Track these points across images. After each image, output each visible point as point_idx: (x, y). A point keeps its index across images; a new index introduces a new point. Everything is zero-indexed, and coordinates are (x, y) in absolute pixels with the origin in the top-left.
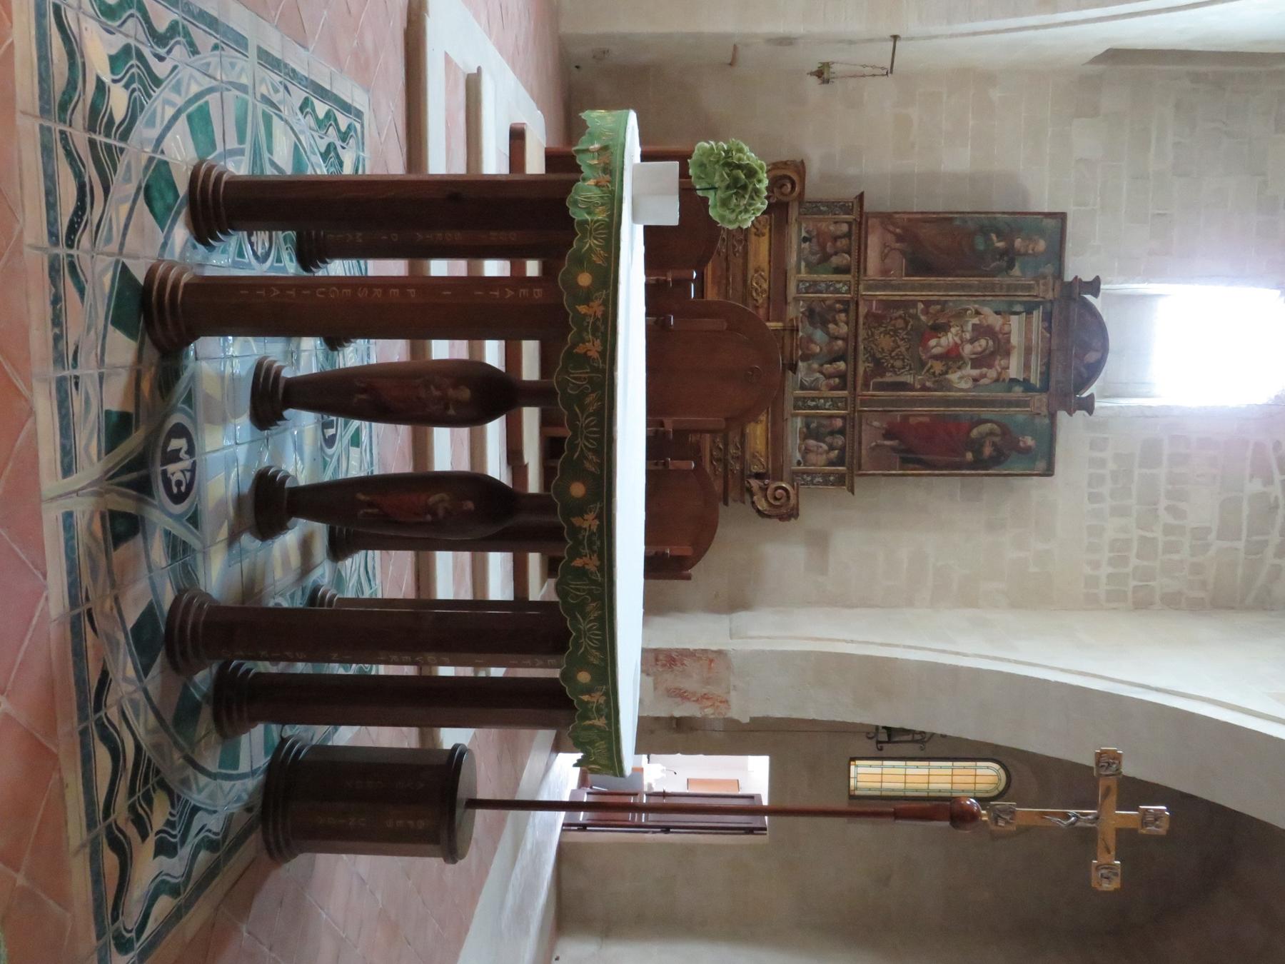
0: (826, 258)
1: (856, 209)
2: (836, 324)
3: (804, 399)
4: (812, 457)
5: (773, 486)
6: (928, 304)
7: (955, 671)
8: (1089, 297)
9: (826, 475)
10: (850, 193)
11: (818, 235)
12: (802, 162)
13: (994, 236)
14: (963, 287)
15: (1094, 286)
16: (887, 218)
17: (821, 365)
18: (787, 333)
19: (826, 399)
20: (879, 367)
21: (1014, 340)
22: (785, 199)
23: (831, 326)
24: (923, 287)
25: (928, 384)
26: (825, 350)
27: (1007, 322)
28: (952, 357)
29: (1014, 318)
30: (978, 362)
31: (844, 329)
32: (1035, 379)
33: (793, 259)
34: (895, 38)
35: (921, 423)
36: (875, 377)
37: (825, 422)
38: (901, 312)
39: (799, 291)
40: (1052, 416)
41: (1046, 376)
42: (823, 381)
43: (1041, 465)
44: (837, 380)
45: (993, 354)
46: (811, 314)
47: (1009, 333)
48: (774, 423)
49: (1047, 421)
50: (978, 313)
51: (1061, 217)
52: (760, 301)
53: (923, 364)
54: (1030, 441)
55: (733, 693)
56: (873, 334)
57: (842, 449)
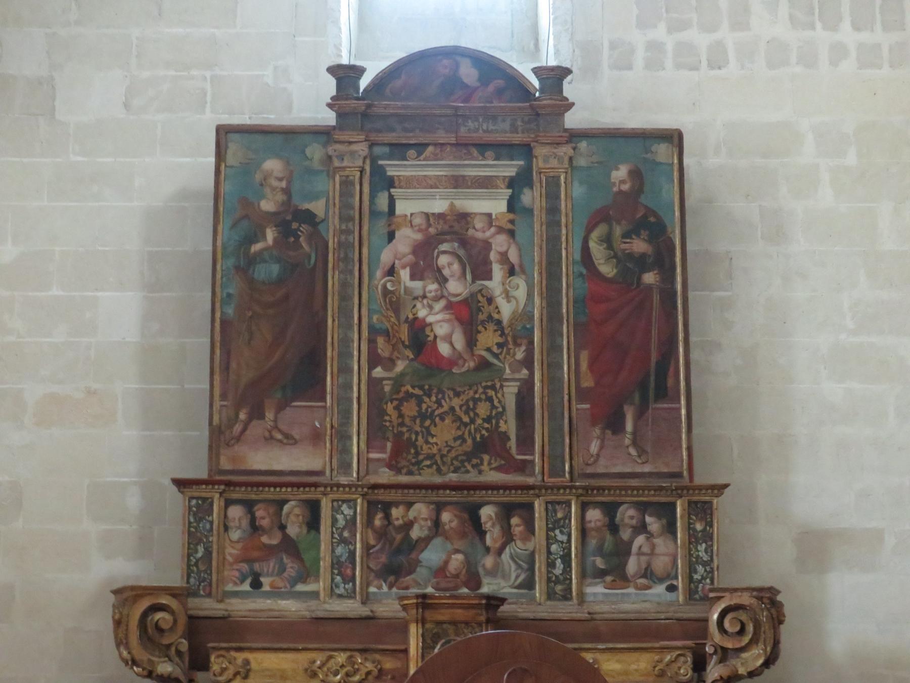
0: (289, 546)
1: (203, 492)
2: (409, 525)
3: (550, 580)
4: (660, 564)
6: (374, 360)
8: (364, 82)
9: (693, 538)
10: (175, 503)
11: (249, 561)
12: (116, 592)
13: (256, 247)
14: (345, 298)
15: (346, 75)
16: (220, 437)
17: (488, 550)
18: (428, 614)
20: (489, 445)
21: (439, 206)
22: (182, 621)
23: (415, 533)
24: (344, 370)
25: (520, 355)
26: (459, 544)
27: (408, 221)
29: (402, 208)
31: (421, 510)
32: (509, 168)
33: (290, 607)
35: (591, 366)
36: (508, 451)
37: (593, 543)
38: (390, 408)
39: (351, 595)
40: (575, 136)
41: (503, 150)
42: (518, 547)
43: (662, 151)
44: (515, 521)
46: (394, 571)
47: (427, 215)
48: (596, 637)
49: (583, 145)
50: (391, 271)
51: (224, 133)
52: (370, 666)
53: (484, 365)
54: (621, 173)
56: (430, 457)
57: (643, 507)
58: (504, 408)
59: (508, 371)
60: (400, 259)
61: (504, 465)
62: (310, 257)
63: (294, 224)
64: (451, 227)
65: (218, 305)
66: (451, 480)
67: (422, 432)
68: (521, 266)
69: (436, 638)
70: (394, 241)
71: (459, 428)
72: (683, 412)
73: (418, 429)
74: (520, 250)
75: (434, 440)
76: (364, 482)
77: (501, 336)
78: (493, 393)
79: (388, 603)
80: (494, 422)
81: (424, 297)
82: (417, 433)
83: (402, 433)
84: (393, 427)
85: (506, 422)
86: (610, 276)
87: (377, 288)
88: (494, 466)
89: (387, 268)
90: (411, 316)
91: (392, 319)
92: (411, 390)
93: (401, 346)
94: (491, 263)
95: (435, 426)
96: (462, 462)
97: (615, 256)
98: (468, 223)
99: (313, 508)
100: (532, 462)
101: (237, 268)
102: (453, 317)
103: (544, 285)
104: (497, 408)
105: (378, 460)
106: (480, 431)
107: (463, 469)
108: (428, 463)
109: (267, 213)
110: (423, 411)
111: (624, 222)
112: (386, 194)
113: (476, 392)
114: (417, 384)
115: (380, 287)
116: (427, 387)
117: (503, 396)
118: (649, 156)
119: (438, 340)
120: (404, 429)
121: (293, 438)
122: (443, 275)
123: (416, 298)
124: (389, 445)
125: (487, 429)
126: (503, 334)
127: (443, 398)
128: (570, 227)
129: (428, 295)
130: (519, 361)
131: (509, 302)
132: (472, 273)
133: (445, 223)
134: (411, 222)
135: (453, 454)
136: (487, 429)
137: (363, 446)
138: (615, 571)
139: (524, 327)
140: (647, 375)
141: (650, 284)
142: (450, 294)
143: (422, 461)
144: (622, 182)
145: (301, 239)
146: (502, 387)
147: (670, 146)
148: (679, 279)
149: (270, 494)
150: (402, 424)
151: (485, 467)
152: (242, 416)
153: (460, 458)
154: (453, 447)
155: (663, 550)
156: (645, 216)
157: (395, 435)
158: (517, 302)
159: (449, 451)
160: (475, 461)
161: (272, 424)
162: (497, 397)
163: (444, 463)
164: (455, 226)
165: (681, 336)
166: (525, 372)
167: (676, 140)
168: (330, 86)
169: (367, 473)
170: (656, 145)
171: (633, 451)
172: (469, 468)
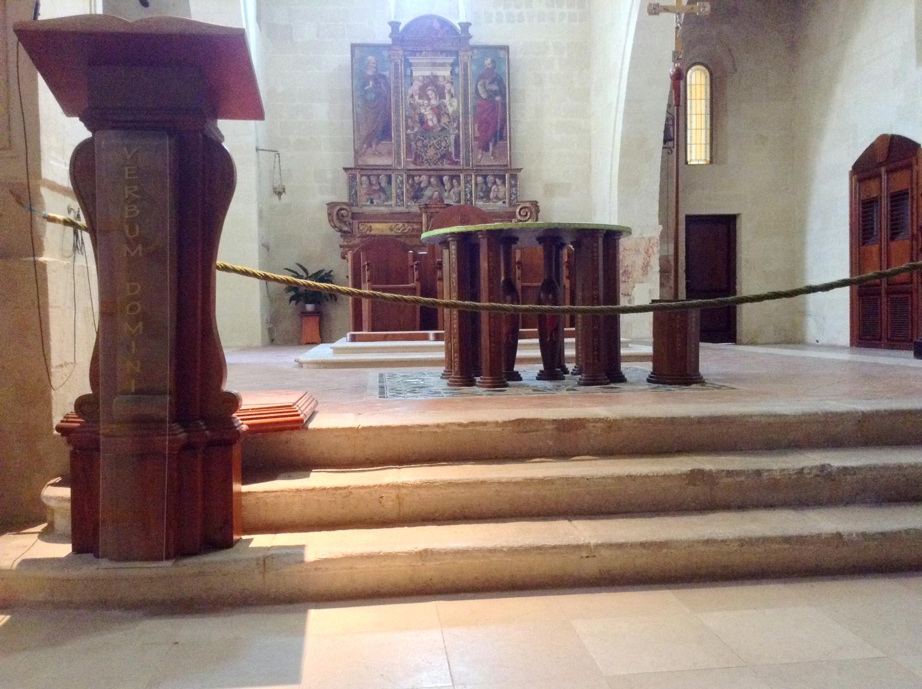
0: (382, 190)
1: (353, 172)
2: (421, 182)
4: (501, 195)
5: (519, 217)
6: (407, 127)
7: (628, 101)
8: (401, 28)
9: (511, 186)
10: (344, 176)
11: (370, 195)
12: (328, 204)
13: (366, 88)
15: (394, 25)
16: (357, 153)
19: (466, 187)
21: (428, 73)
22: (350, 215)
23: (422, 185)
24: (398, 131)
25: (455, 125)
28: (439, 111)
29: (415, 74)
30: (441, 96)
31: (424, 178)
32: (451, 60)
33: (383, 209)
34: (257, 150)
35: (478, 130)
37: (479, 188)
38: (413, 143)
39: (403, 205)
41: (448, 53)
42: (456, 190)
43: (502, 54)
45: (436, 86)
46: (416, 198)
50: (412, 96)
51: (353, 46)
53: (443, 129)
54: (488, 62)
55: (644, 235)
57: (495, 176)
69: (431, 217)
79: (415, 208)
99: (389, 177)
138: (486, 196)
149: (375, 172)
155: (500, 190)
164: (433, 81)
168: (389, 30)
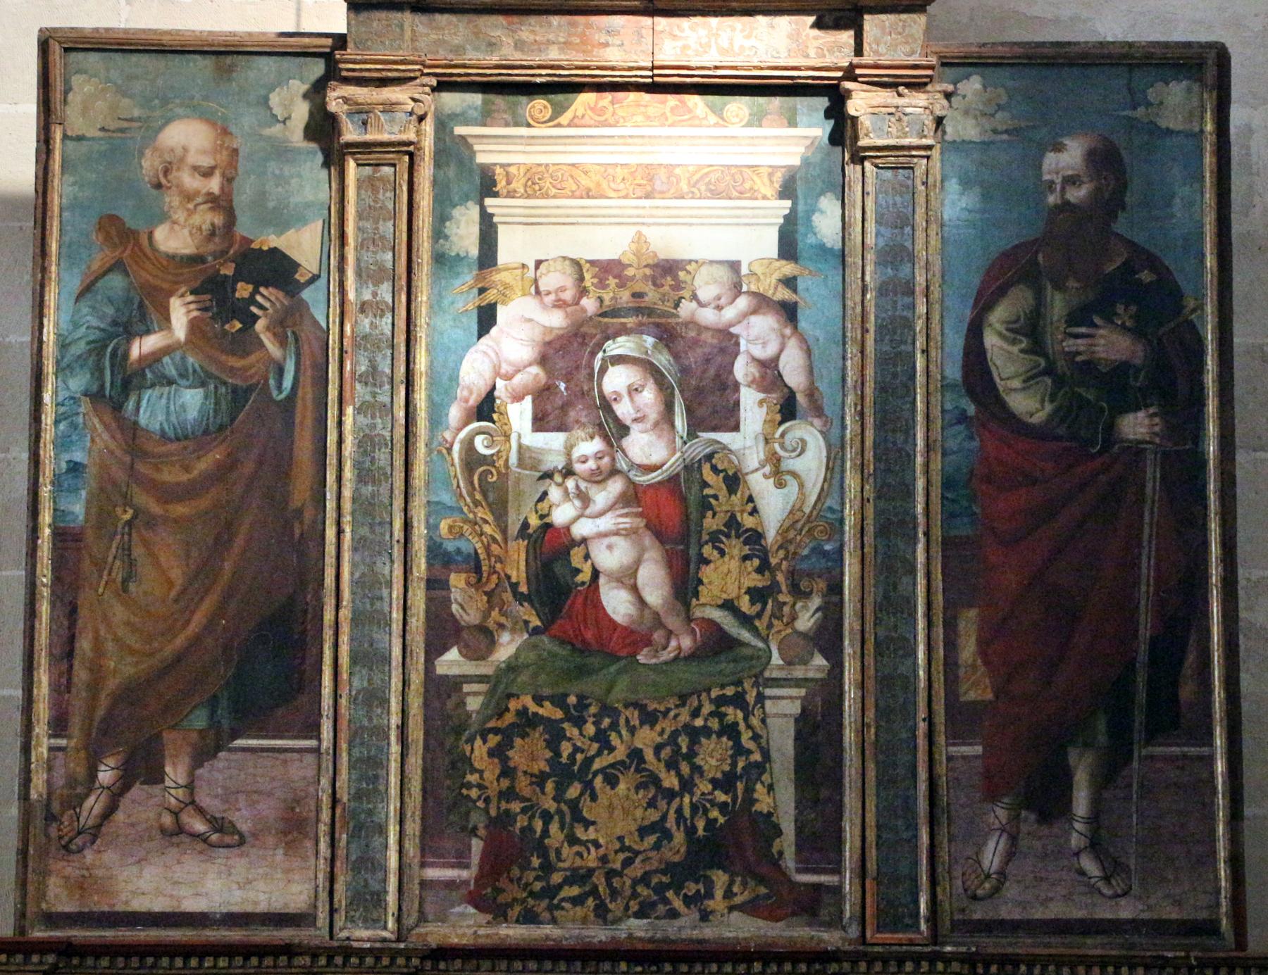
6: (443, 630)
13: (143, 346)
16: (51, 828)
20: (731, 844)
25: (806, 620)
29: (513, 247)
36: (775, 862)
38: (479, 751)
43: (1175, 101)
50: (486, 408)
51: (59, 52)
53: (717, 644)
54: (1070, 156)
56: (579, 876)
58: (766, 755)
59: (776, 659)
60: (508, 377)
61: (768, 897)
62: (280, 371)
63: (240, 285)
64: (637, 295)
65: (46, 491)
66: (630, 936)
67: (559, 811)
68: (812, 393)
70: (494, 331)
71: (652, 804)
72: (1220, 766)
73: (551, 805)
74: (809, 353)
75: (591, 834)
76: (413, 941)
77: (759, 570)
78: (740, 715)
80: (740, 786)
81: (568, 472)
82: (547, 817)
83: (508, 817)
84: (487, 801)
85: (771, 788)
86: (1036, 420)
87: (449, 450)
88: (738, 900)
89: (474, 401)
90: (534, 521)
91: (488, 529)
92: (533, 708)
93: (508, 596)
94: (737, 386)
95: (594, 798)
96: (660, 889)
97: (1049, 371)
98: (678, 286)
100: (837, 890)
101: (96, 396)
102: (641, 523)
103: (869, 442)
104: (749, 752)
105: (450, 885)
106: (706, 811)
107: (661, 909)
108: (575, 891)
109: (171, 257)
110: (564, 760)
111: (1072, 283)
112: (474, 212)
113: (696, 713)
114: (547, 691)
115: (456, 447)
116: (572, 700)
117: (763, 721)
118: (1141, 111)
119: (602, 580)
120: (516, 807)
121: (234, 830)
122: (617, 420)
123: (548, 475)
124: (477, 845)
125: (723, 807)
126: (764, 568)
127: (614, 726)
128: (936, 294)
129: (578, 467)
130: (800, 634)
131: (780, 485)
132: (689, 411)
133: (621, 285)
134: (536, 281)
135: (637, 870)
136: (723, 807)
137: (412, 849)
139: (818, 551)
140: (1131, 666)
141: (1139, 442)
142: (633, 465)
143: (560, 887)
144: (1071, 181)
145: (260, 325)
146: (761, 698)
147: (1196, 87)
148: (1212, 429)
150: (509, 794)
151: (717, 903)
152: (106, 775)
153: (655, 880)
154: (637, 853)
156: (1128, 269)
157: (493, 823)
158: (801, 486)
159: (627, 863)
160: (691, 888)
161: (180, 793)
162: (749, 727)
163: (614, 893)
165: (1215, 573)
166: (819, 661)
167: (1211, 73)
169: (422, 918)
170: (1159, 85)
171: (1089, 865)
172: (678, 904)
